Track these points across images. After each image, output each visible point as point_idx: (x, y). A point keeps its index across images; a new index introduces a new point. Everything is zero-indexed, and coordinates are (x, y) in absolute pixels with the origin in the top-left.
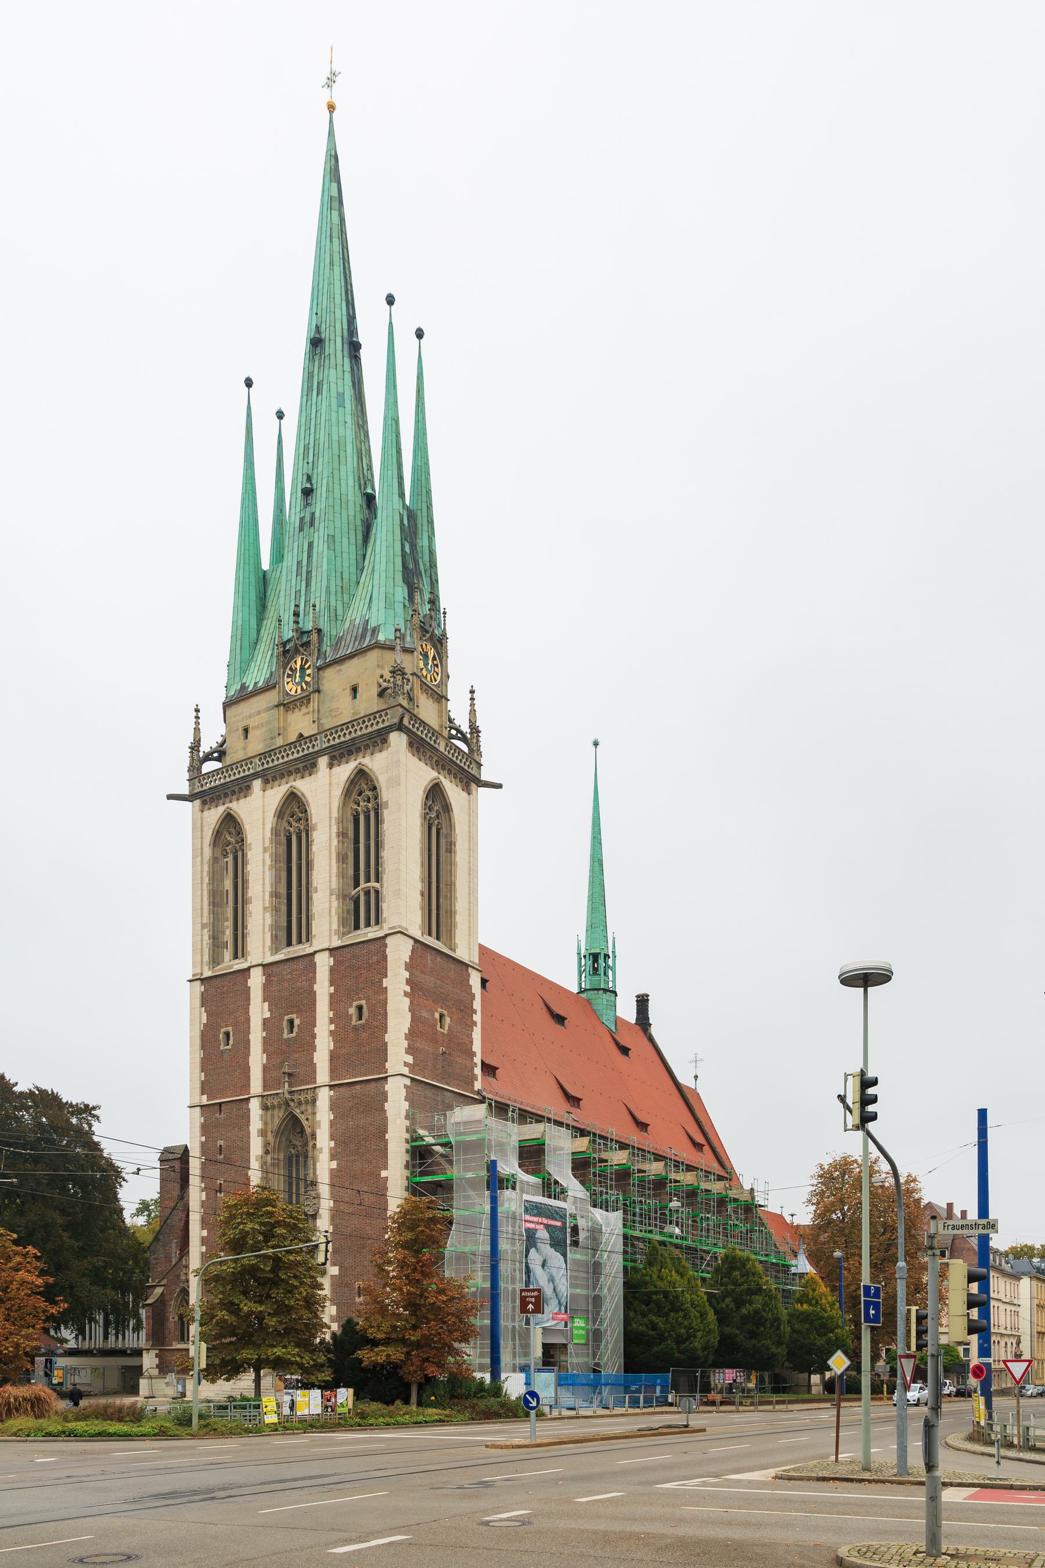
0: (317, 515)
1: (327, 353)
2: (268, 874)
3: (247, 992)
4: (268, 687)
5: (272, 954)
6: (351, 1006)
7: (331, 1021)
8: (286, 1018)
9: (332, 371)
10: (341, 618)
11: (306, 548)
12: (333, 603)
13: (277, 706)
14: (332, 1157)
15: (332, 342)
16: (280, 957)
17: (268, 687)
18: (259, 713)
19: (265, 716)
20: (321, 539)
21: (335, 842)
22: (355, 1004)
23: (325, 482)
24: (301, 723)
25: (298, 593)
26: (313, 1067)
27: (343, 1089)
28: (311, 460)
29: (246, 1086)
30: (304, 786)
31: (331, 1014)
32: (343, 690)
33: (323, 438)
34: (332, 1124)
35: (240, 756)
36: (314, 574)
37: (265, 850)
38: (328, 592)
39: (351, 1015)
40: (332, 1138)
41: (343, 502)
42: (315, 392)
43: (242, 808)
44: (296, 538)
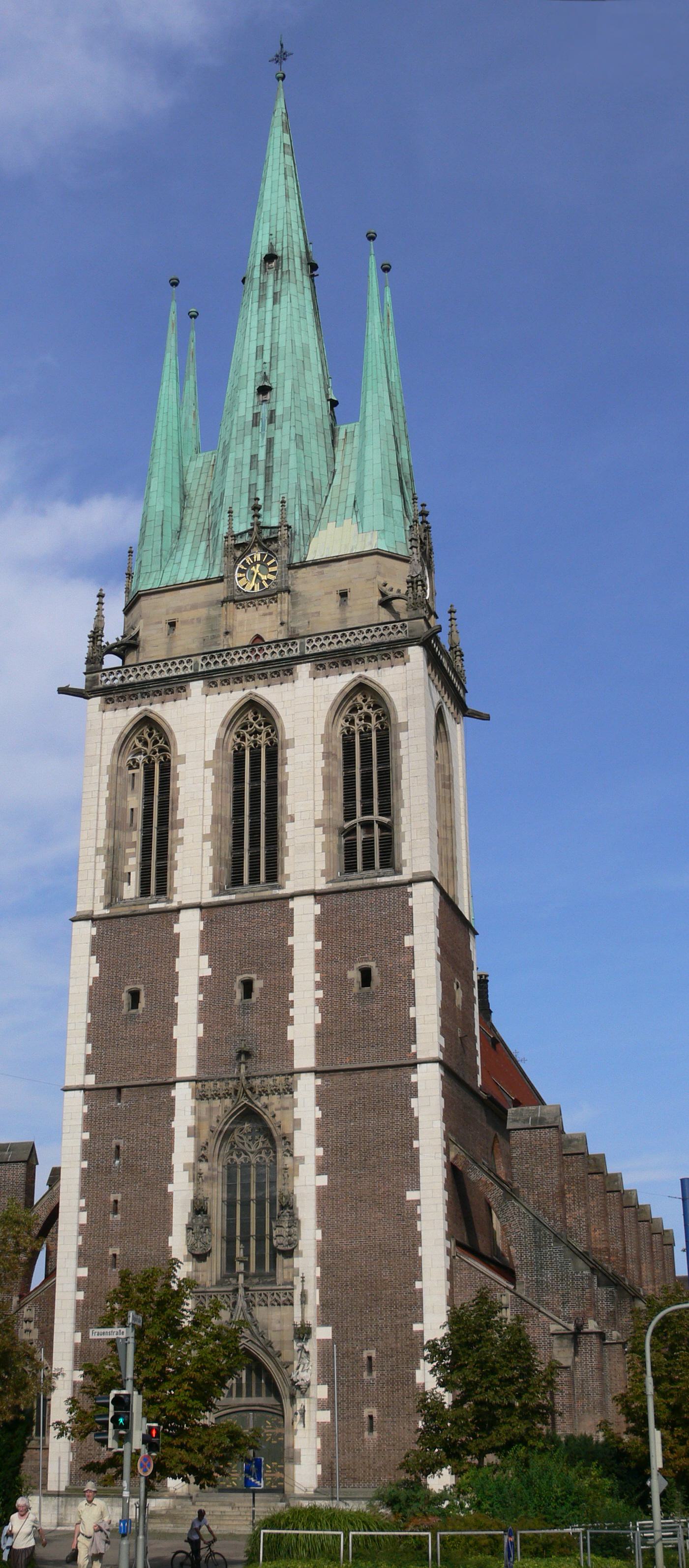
0: (279, 412)
1: (285, 268)
2: (209, 794)
3: (173, 945)
5: (214, 895)
6: (351, 968)
7: (318, 986)
8: (239, 978)
10: (314, 518)
11: (263, 442)
13: (223, 602)
14: (320, 1171)
15: (291, 261)
18: (194, 607)
20: (286, 439)
21: (322, 763)
23: (288, 384)
25: (252, 487)
27: (338, 1078)
28: (267, 358)
29: (171, 1064)
31: (318, 977)
32: (327, 593)
33: (282, 341)
35: (159, 653)
36: (276, 469)
38: (298, 488)
39: (352, 980)
40: (319, 1143)
41: (310, 406)
42: (270, 301)
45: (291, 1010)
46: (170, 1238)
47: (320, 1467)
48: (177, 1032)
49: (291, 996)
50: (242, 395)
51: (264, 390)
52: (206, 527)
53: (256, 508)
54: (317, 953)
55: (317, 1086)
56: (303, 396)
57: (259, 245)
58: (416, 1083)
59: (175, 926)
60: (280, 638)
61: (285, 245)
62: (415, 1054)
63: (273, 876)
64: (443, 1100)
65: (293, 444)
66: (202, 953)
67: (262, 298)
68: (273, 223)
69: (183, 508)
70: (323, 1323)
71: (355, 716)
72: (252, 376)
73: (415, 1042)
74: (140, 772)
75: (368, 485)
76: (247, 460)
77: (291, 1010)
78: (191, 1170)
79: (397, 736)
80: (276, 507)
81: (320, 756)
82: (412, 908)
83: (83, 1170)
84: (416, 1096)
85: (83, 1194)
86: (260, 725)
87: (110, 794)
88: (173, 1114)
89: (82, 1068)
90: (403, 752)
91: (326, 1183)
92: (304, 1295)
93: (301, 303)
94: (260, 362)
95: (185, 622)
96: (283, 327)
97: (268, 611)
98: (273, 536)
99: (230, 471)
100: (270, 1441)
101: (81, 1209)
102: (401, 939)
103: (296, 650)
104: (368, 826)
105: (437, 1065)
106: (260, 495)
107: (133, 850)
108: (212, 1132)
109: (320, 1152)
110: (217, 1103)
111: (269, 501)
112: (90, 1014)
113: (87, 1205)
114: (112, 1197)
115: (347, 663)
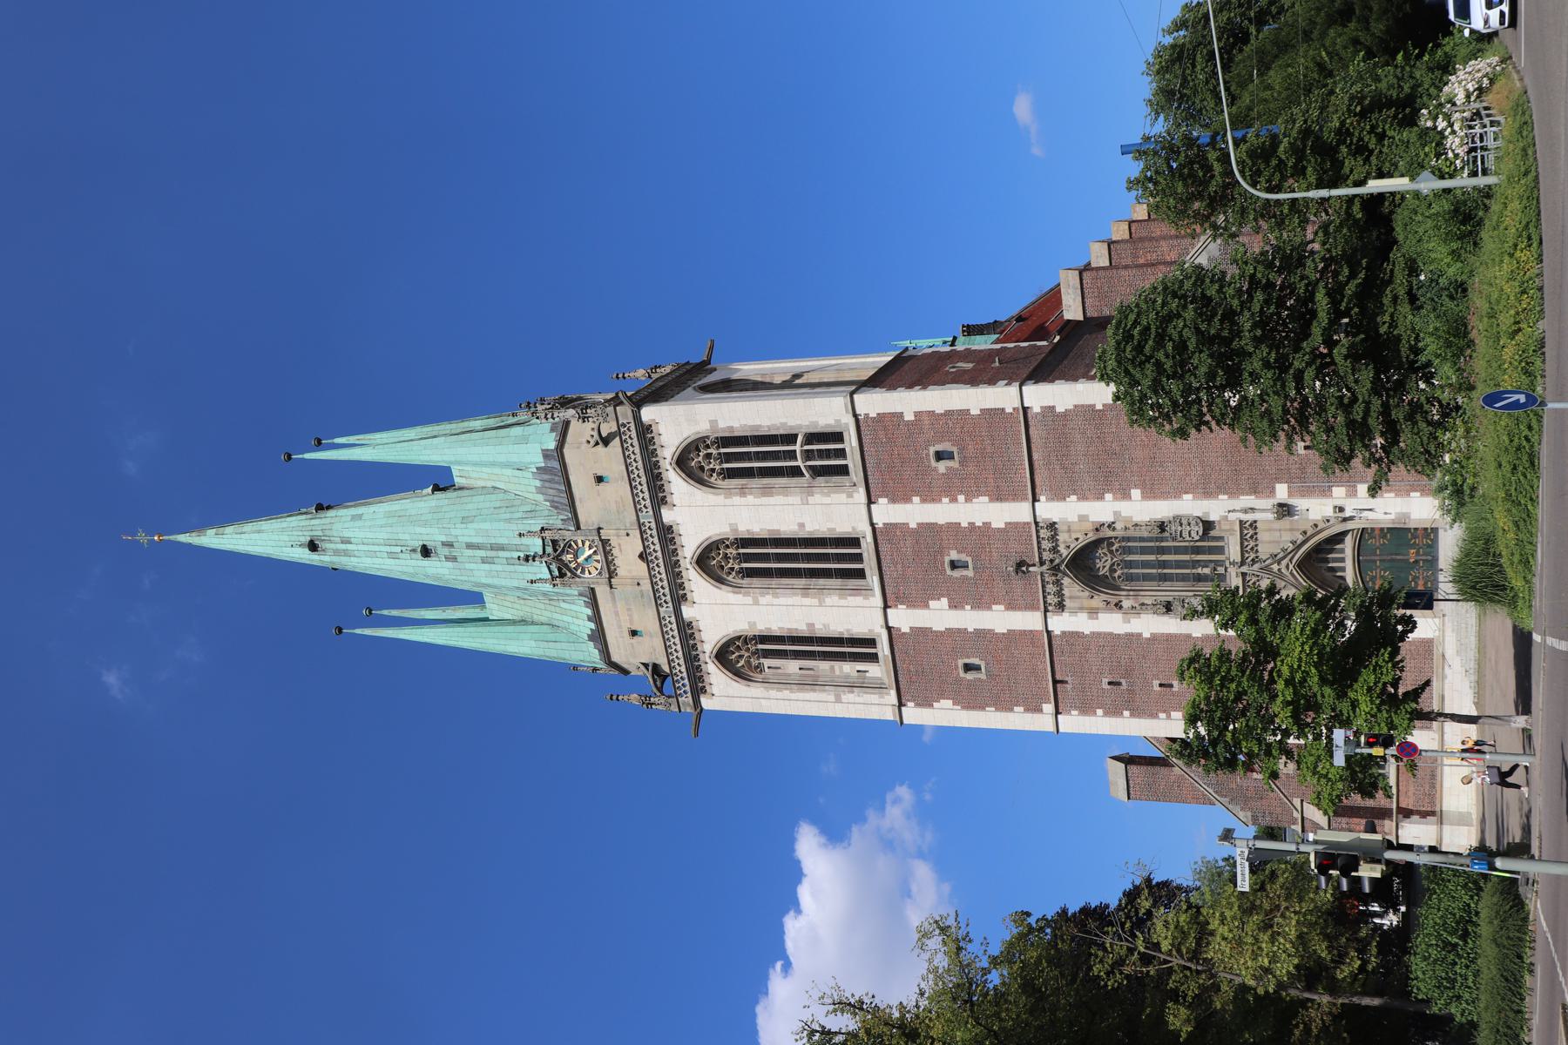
0: (444, 539)
1: (320, 533)
2: (782, 600)
3: (921, 633)
4: (594, 603)
5: (874, 596)
6: (935, 469)
7: (954, 500)
9: (334, 527)
11: (470, 552)
12: (519, 515)
13: (611, 587)
16: (873, 580)
17: (594, 603)
18: (617, 614)
19: (620, 605)
20: (466, 532)
21: (750, 499)
22: (933, 463)
23: (418, 530)
24: (627, 552)
25: (509, 561)
26: (1012, 526)
28: (398, 549)
30: (689, 545)
31: (945, 500)
32: (599, 495)
33: (382, 535)
34: (1083, 498)
37: (756, 603)
38: (509, 521)
39: (947, 468)
40: (1100, 497)
42: (349, 547)
43: (710, 638)
44: (461, 566)
45: (977, 525)
46: (1194, 635)
47: (1412, 494)
48: (1001, 629)
49: (964, 524)
50: (430, 571)
51: (426, 552)
52: (548, 602)
53: (527, 559)
54: (923, 501)
55: (1048, 500)
56: (429, 517)
57: (302, 556)
58: (1041, 407)
59: (903, 631)
60: (639, 536)
61: (301, 533)
62: (1014, 409)
63: (855, 542)
64: (1057, 381)
65: (470, 525)
66: (927, 606)
67: (346, 553)
68: (282, 544)
69: (533, 623)
70: (1273, 492)
71: (707, 468)
72: (413, 563)
73: (1003, 409)
74: (767, 662)
75: (502, 459)
76: (486, 567)
77: (977, 525)
78: (1129, 616)
79: (723, 430)
80: (525, 541)
81: (743, 500)
82: (878, 414)
83: (1132, 715)
84: (1054, 407)
85: (1154, 716)
86: (720, 554)
87: (786, 689)
88: (1077, 633)
89: (1036, 716)
90: (736, 425)
91: (1139, 491)
92: (1245, 511)
93: (349, 519)
94: (401, 555)
95: (631, 621)
96: (370, 535)
97: (617, 547)
98: (551, 544)
99: (496, 581)
100: (1387, 540)
101: (1169, 717)
102: (908, 423)
103: (649, 522)
104: (808, 455)
105: (1023, 388)
106: (516, 555)
107: (837, 668)
108: (1092, 597)
109: (1109, 496)
110: (1066, 592)
111: (522, 547)
112: (987, 709)
113: (1164, 712)
114: (1156, 688)
115: (659, 477)
